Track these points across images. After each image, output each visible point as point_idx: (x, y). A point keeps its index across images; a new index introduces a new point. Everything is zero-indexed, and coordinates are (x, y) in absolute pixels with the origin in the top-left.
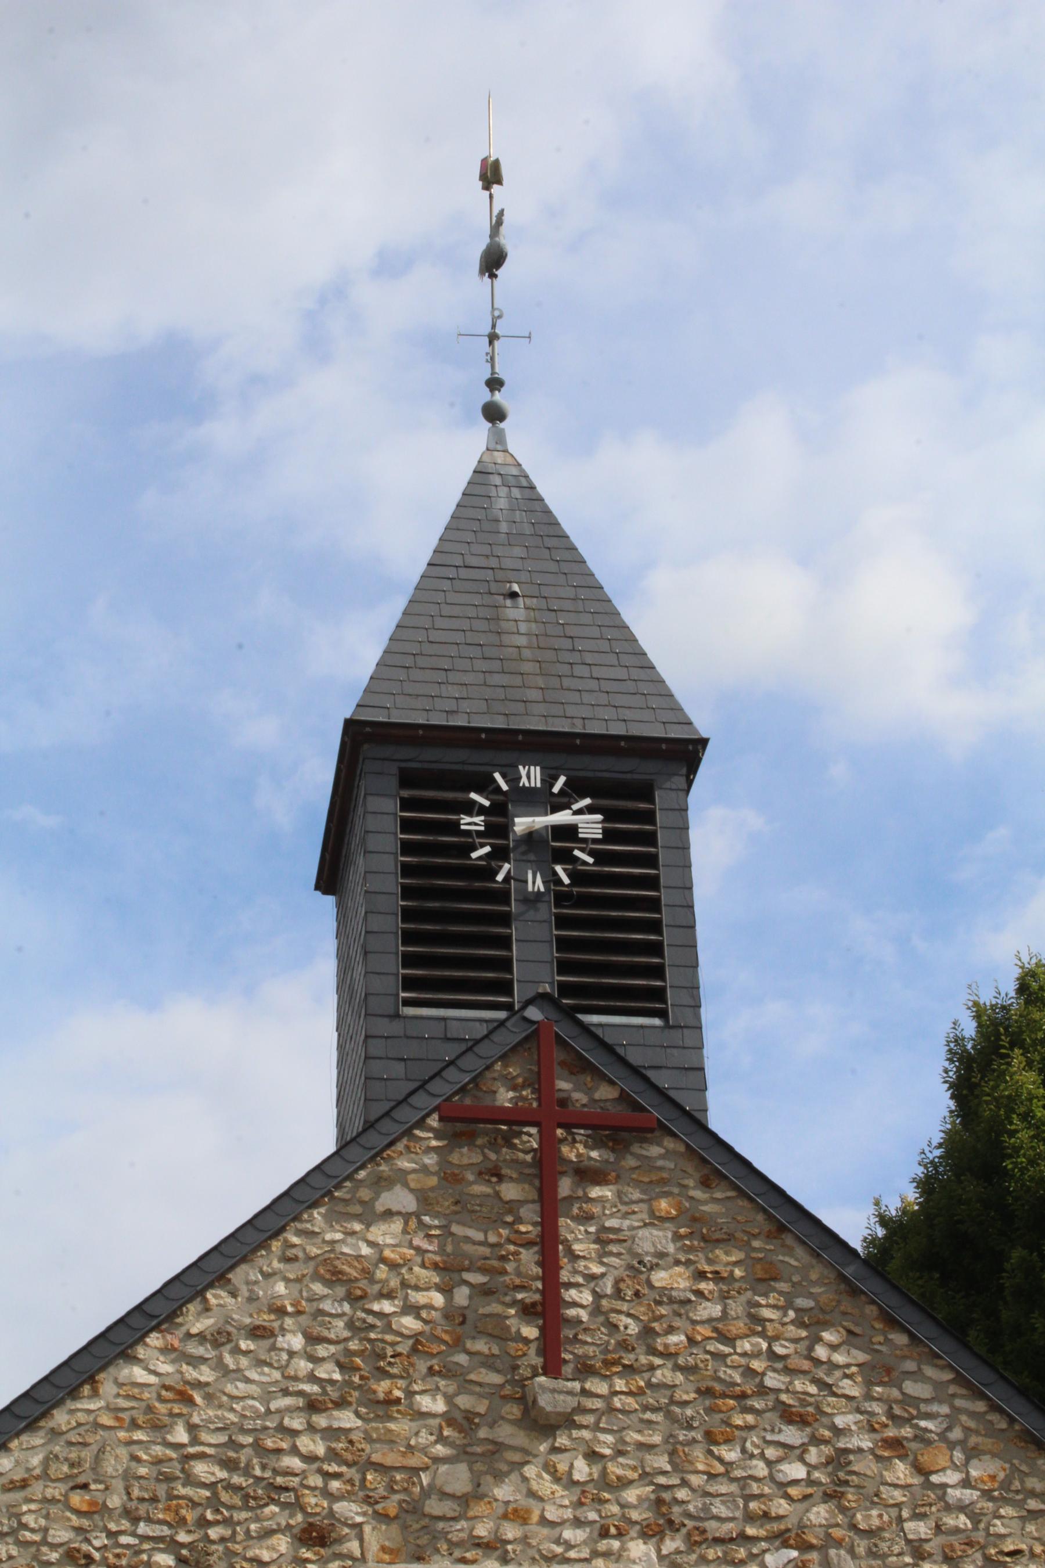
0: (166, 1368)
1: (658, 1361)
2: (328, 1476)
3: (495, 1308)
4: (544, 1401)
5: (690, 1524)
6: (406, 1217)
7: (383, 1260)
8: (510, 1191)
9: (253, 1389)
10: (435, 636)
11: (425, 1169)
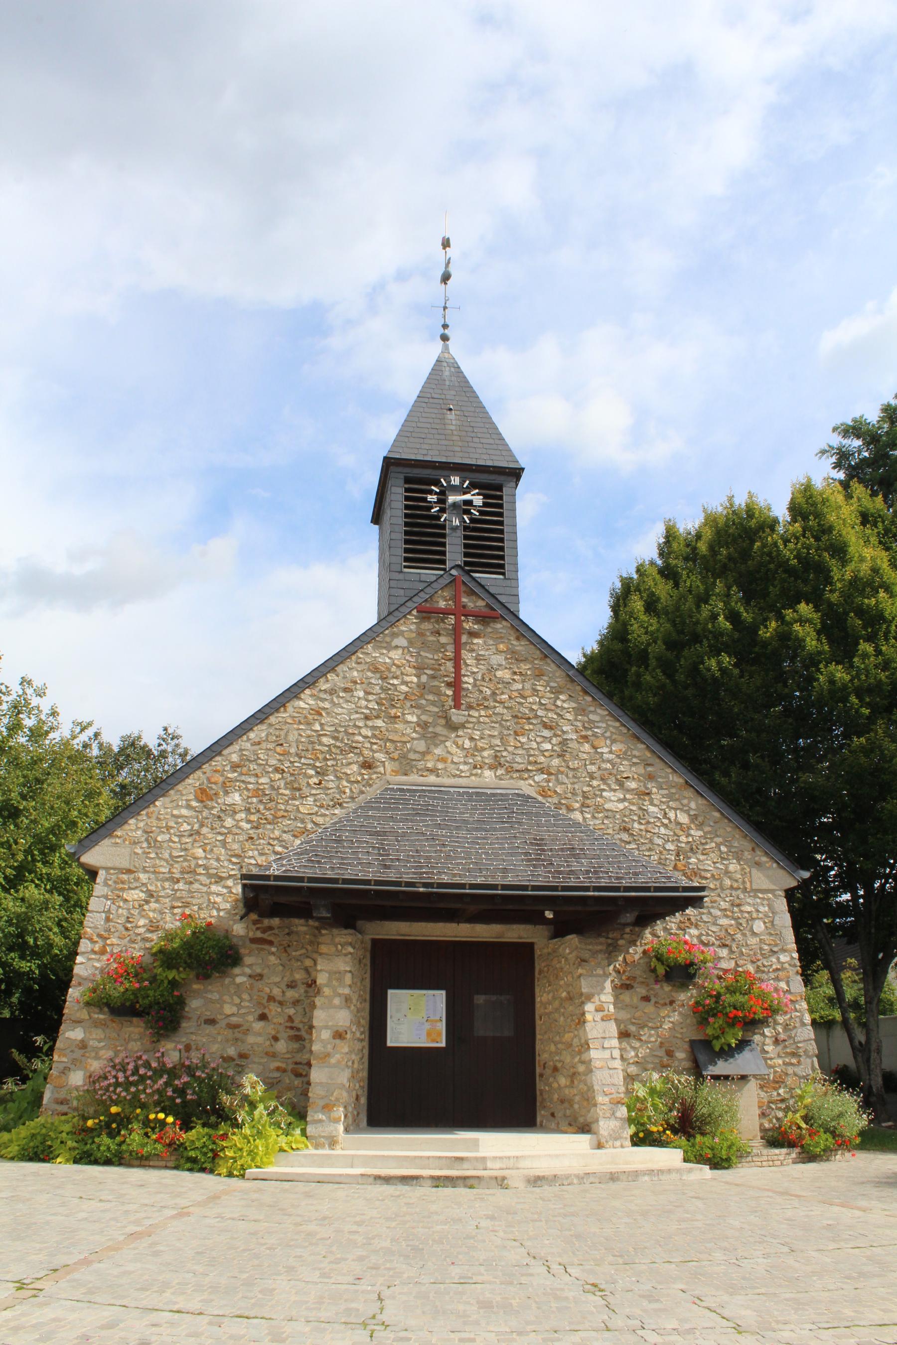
0: (312, 702)
1: (497, 705)
2: (372, 743)
3: (436, 683)
4: (454, 718)
5: (507, 764)
6: (404, 648)
7: (394, 664)
8: (443, 640)
9: (344, 711)
10: (419, 425)
11: (411, 630)
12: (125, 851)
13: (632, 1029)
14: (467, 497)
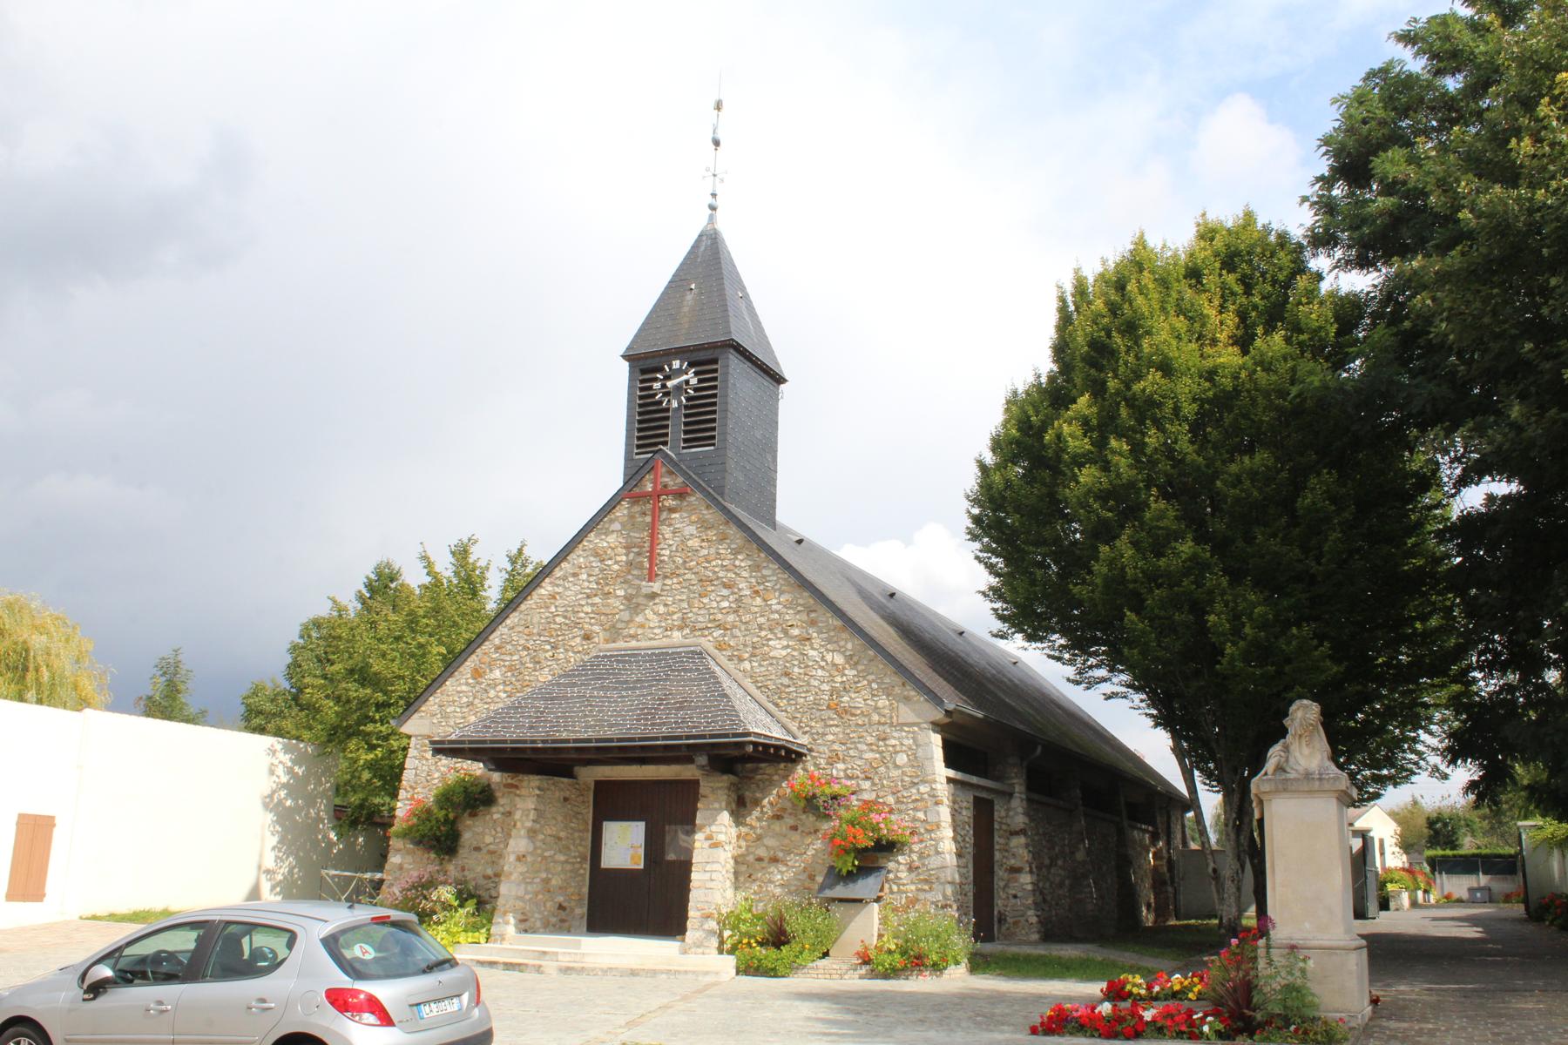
12: (427, 722)
13: (780, 855)
14: (685, 377)
